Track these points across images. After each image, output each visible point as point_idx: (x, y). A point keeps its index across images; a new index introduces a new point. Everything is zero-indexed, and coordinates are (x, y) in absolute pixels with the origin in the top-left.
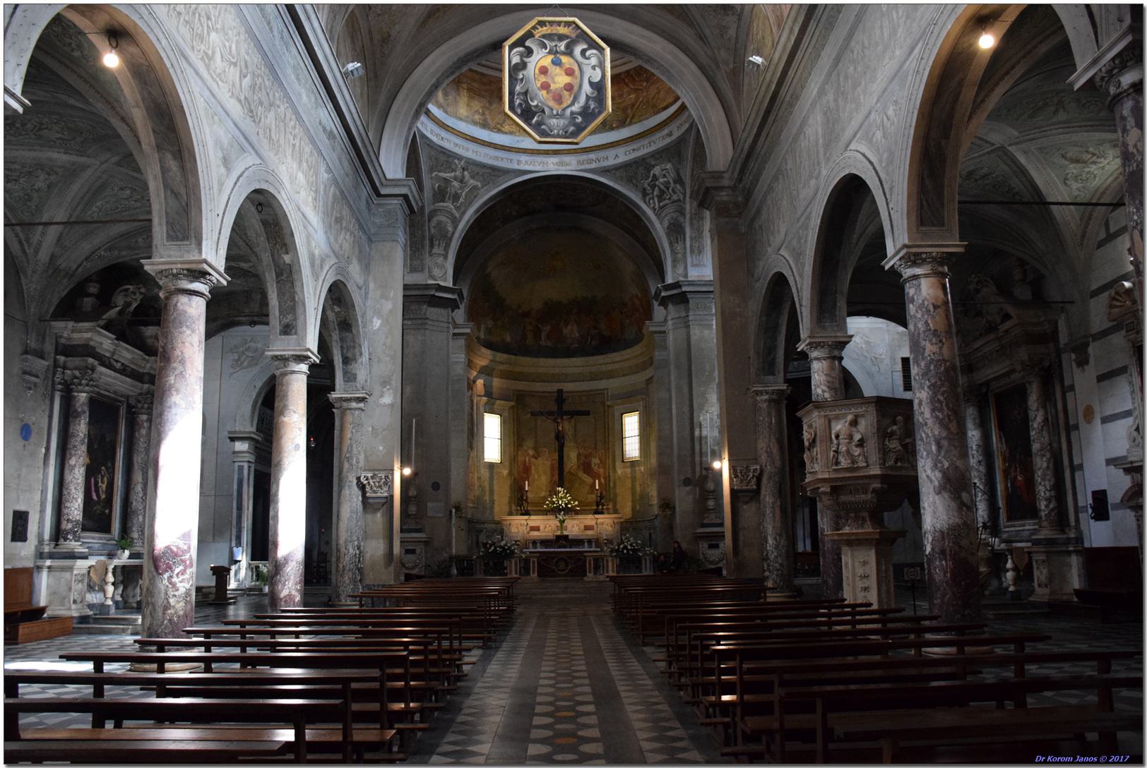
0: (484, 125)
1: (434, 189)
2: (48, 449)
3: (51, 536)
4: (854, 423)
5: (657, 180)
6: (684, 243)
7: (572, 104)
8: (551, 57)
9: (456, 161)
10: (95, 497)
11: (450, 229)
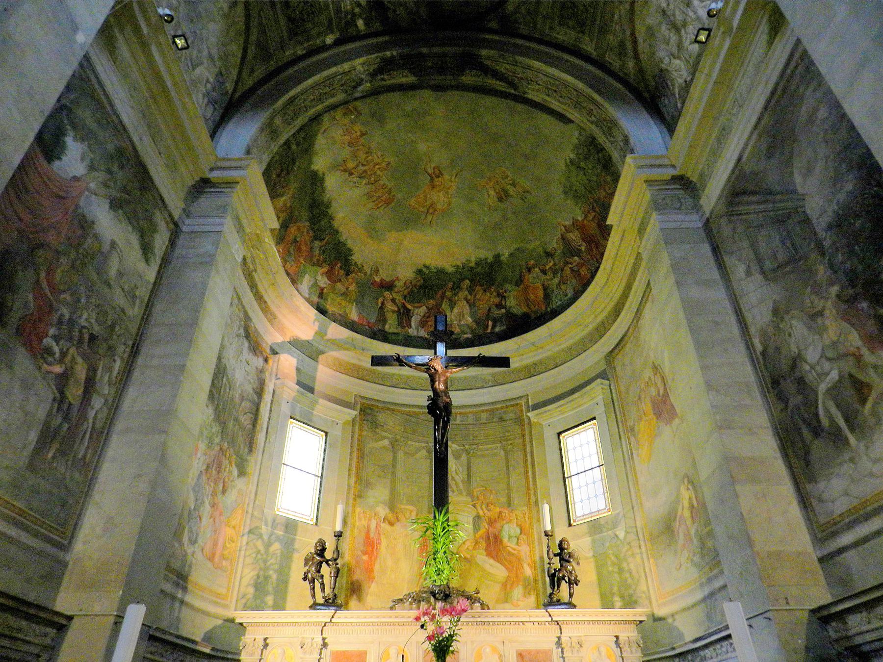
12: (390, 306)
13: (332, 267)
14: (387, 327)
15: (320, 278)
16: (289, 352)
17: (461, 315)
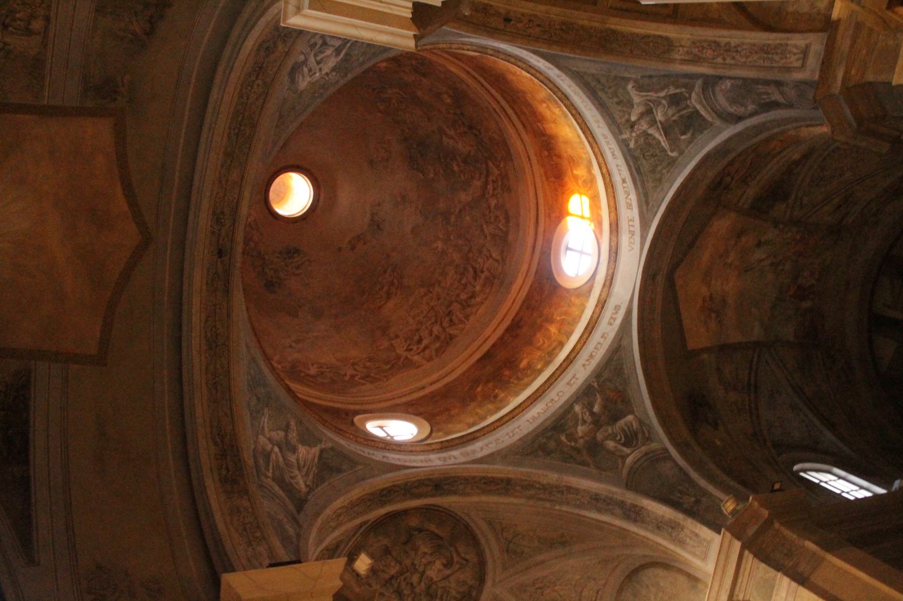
1: (693, 137)
9: (632, 145)
11: (728, 83)
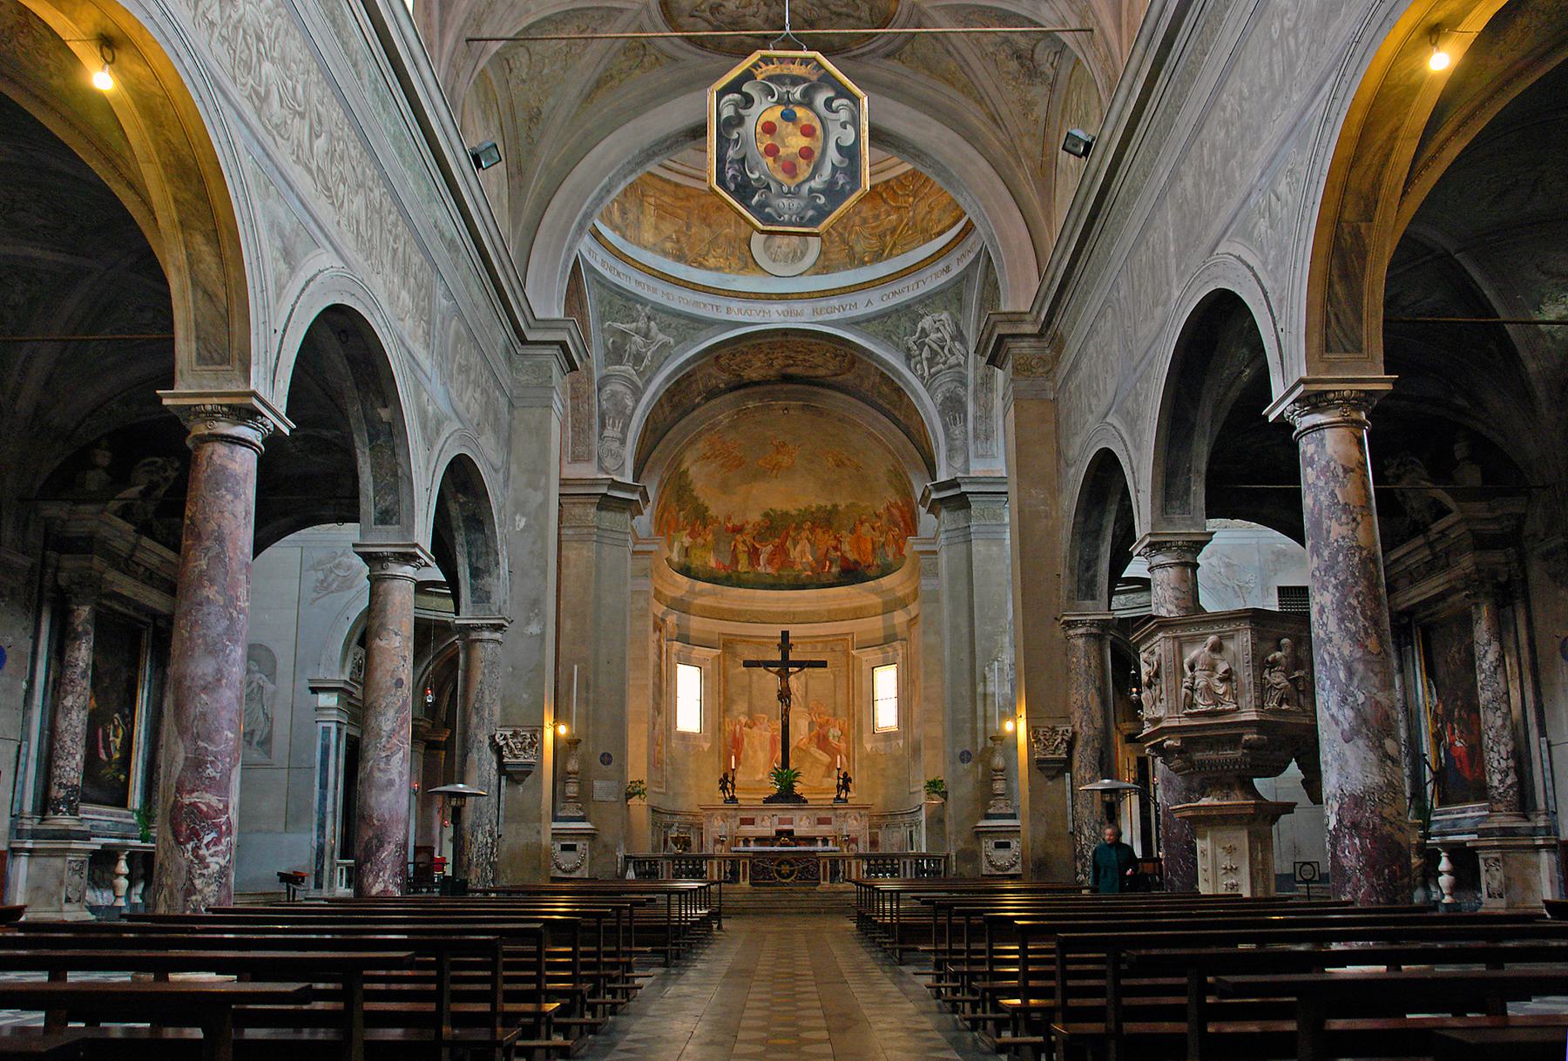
0: (680, 257)
2: (31, 683)
3: (34, 807)
4: (1217, 648)
5: (927, 336)
6: (965, 425)
7: (812, 177)
8: (781, 109)
9: (638, 306)
10: (103, 756)
11: (630, 403)
12: (741, 547)
13: (693, 526)
14: (739, 567)
15: (684, 540)
16: (671, 614)
17: (803, 553)
